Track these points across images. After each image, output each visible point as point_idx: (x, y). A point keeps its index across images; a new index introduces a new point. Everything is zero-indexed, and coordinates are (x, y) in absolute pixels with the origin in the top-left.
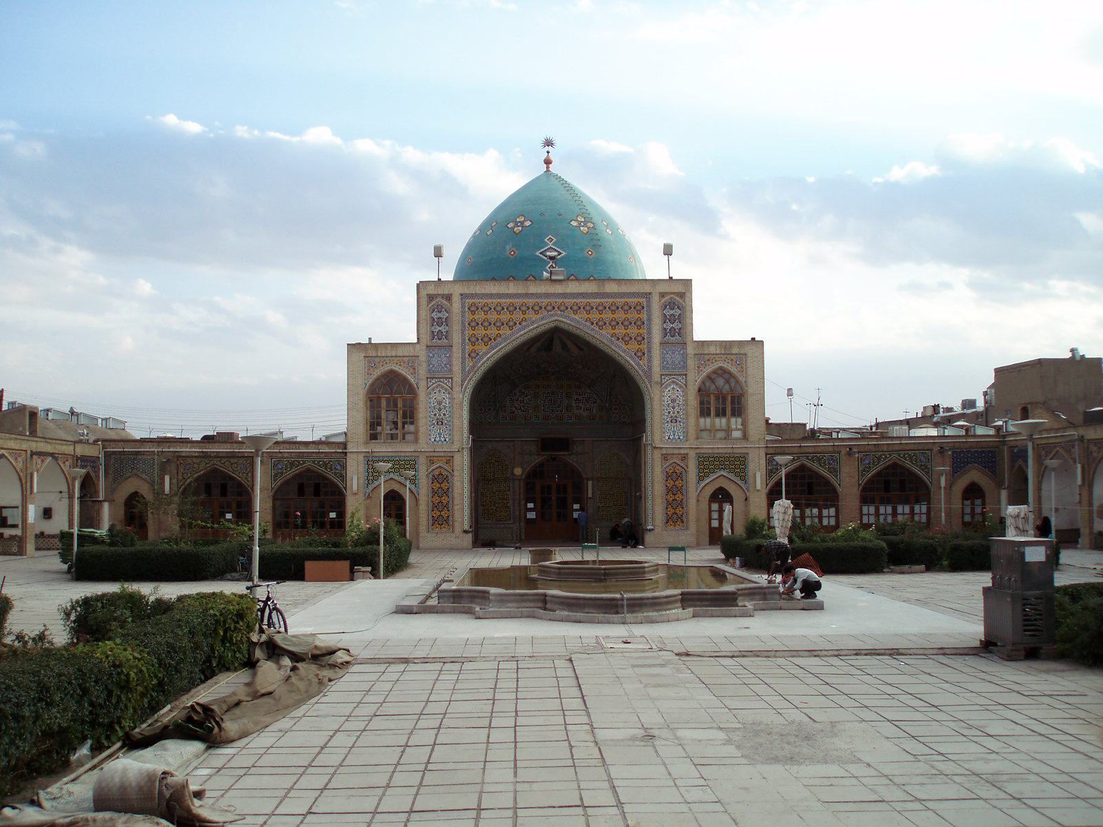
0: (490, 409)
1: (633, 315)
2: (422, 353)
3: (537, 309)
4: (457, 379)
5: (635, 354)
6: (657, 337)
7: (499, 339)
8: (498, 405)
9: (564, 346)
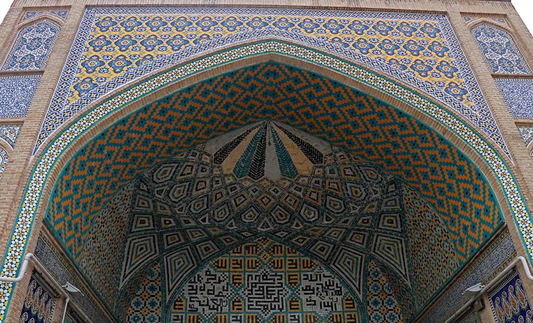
0: (153, 304)
8: (168, 297)
9: (285, 160)
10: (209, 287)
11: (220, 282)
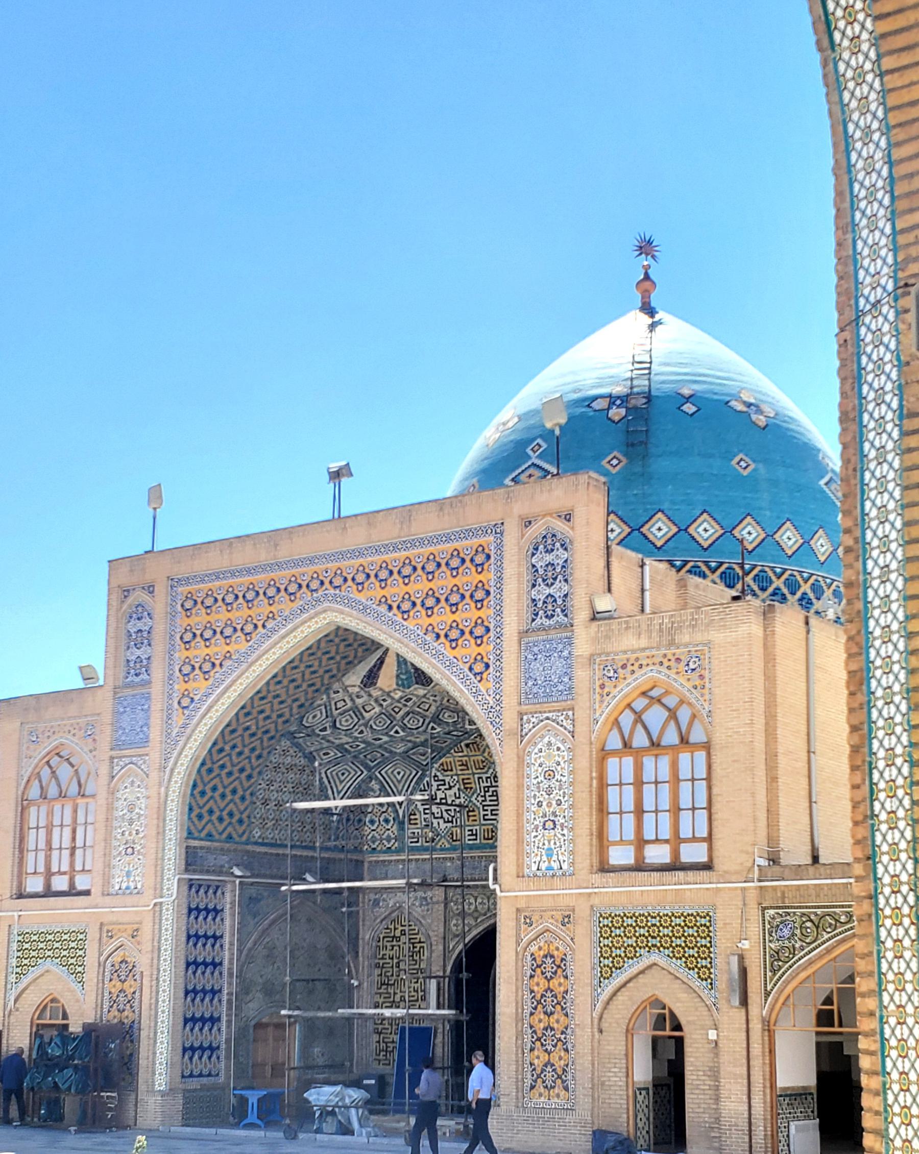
0: (387, 821)
5: (471, 669)
6: (512, 624)
7: (227, 663)
8: (401, 812)
10: (440, 795)
11: (450, 788)
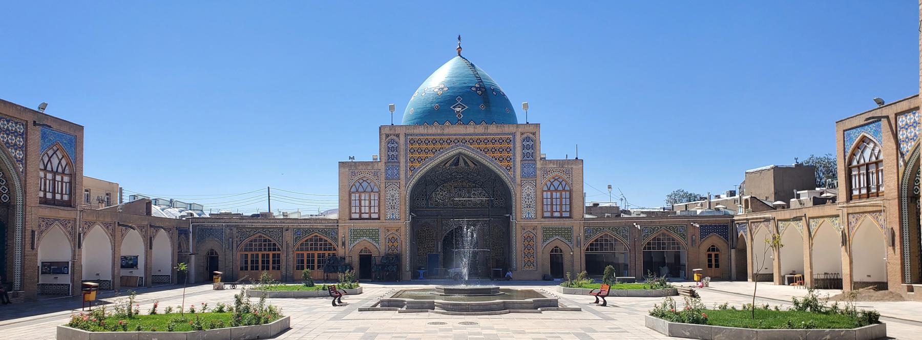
1: (505, 145)
2: (382, 166)
3: (449, 142)
4: (403, 182)
6: (519, 158)
9: (466, 163)
